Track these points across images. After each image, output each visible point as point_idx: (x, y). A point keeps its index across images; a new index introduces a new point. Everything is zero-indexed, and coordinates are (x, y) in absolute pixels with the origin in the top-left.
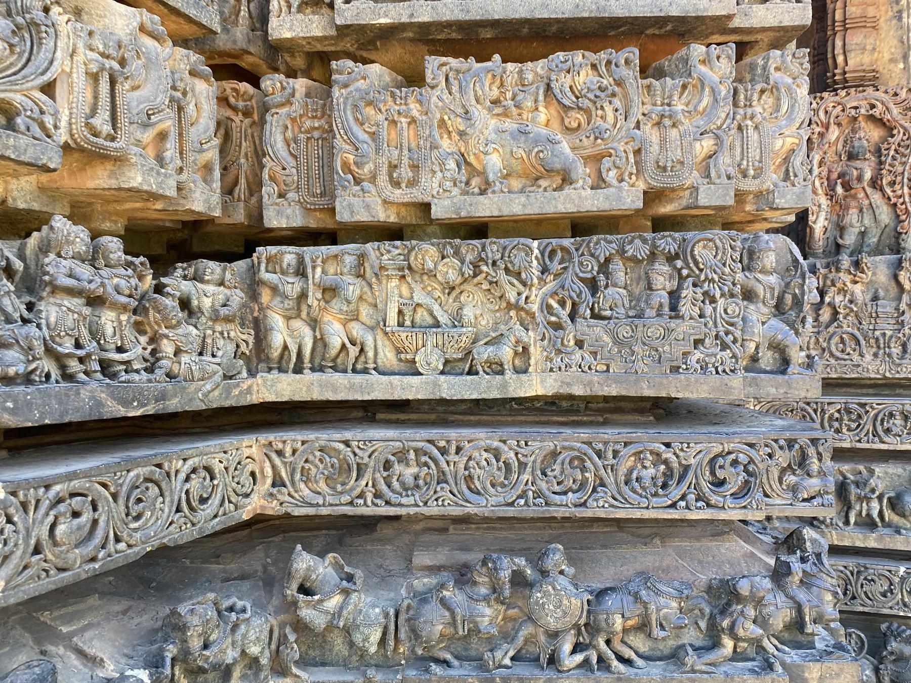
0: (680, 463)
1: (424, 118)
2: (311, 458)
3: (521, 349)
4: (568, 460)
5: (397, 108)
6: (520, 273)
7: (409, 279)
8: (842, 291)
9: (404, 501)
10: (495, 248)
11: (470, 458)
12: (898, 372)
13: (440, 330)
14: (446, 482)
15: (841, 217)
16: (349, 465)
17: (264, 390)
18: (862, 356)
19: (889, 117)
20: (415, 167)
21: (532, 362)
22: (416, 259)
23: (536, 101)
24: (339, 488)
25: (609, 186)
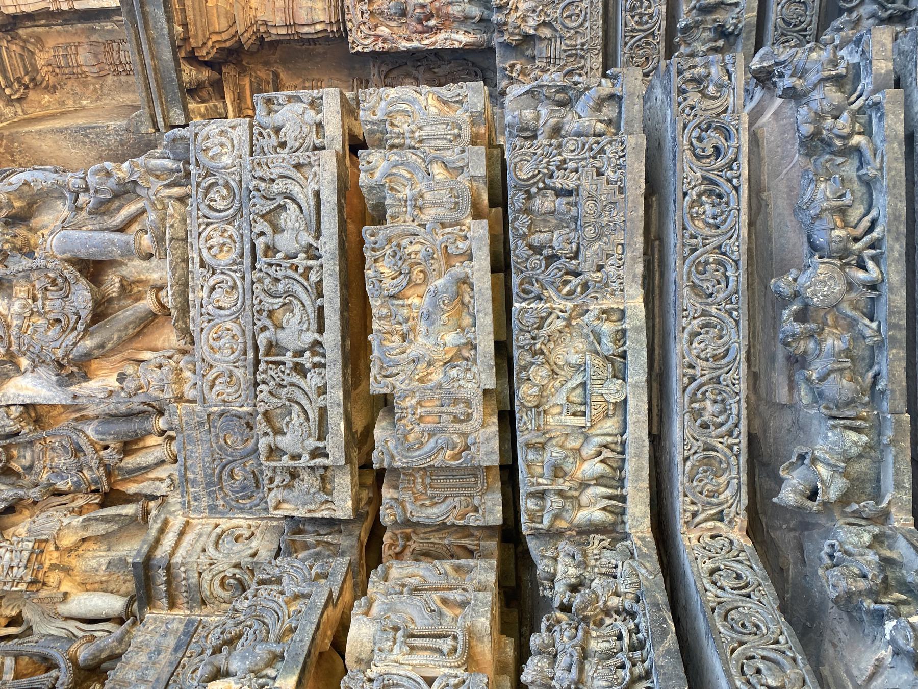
0: (701, 184)
1: (417, 394)
2: (698, 489)
3: (605, 316)
4: (699, 276)
5: (410, 416)
6: (541, 318)
7: (546, 407)
8: (524, 19)
9: (735, 412)
10: (521, 338)
11: (698, 357)
13: (589, 382)
14: (719, 376)
15: (456, 19)
16: (704, 458)
17: (640, 528)
20: (456, 401)
21: (615, 306)
22: (530, 402)
23: (403, 306)
24: (724, 466)
25: (470, 247)
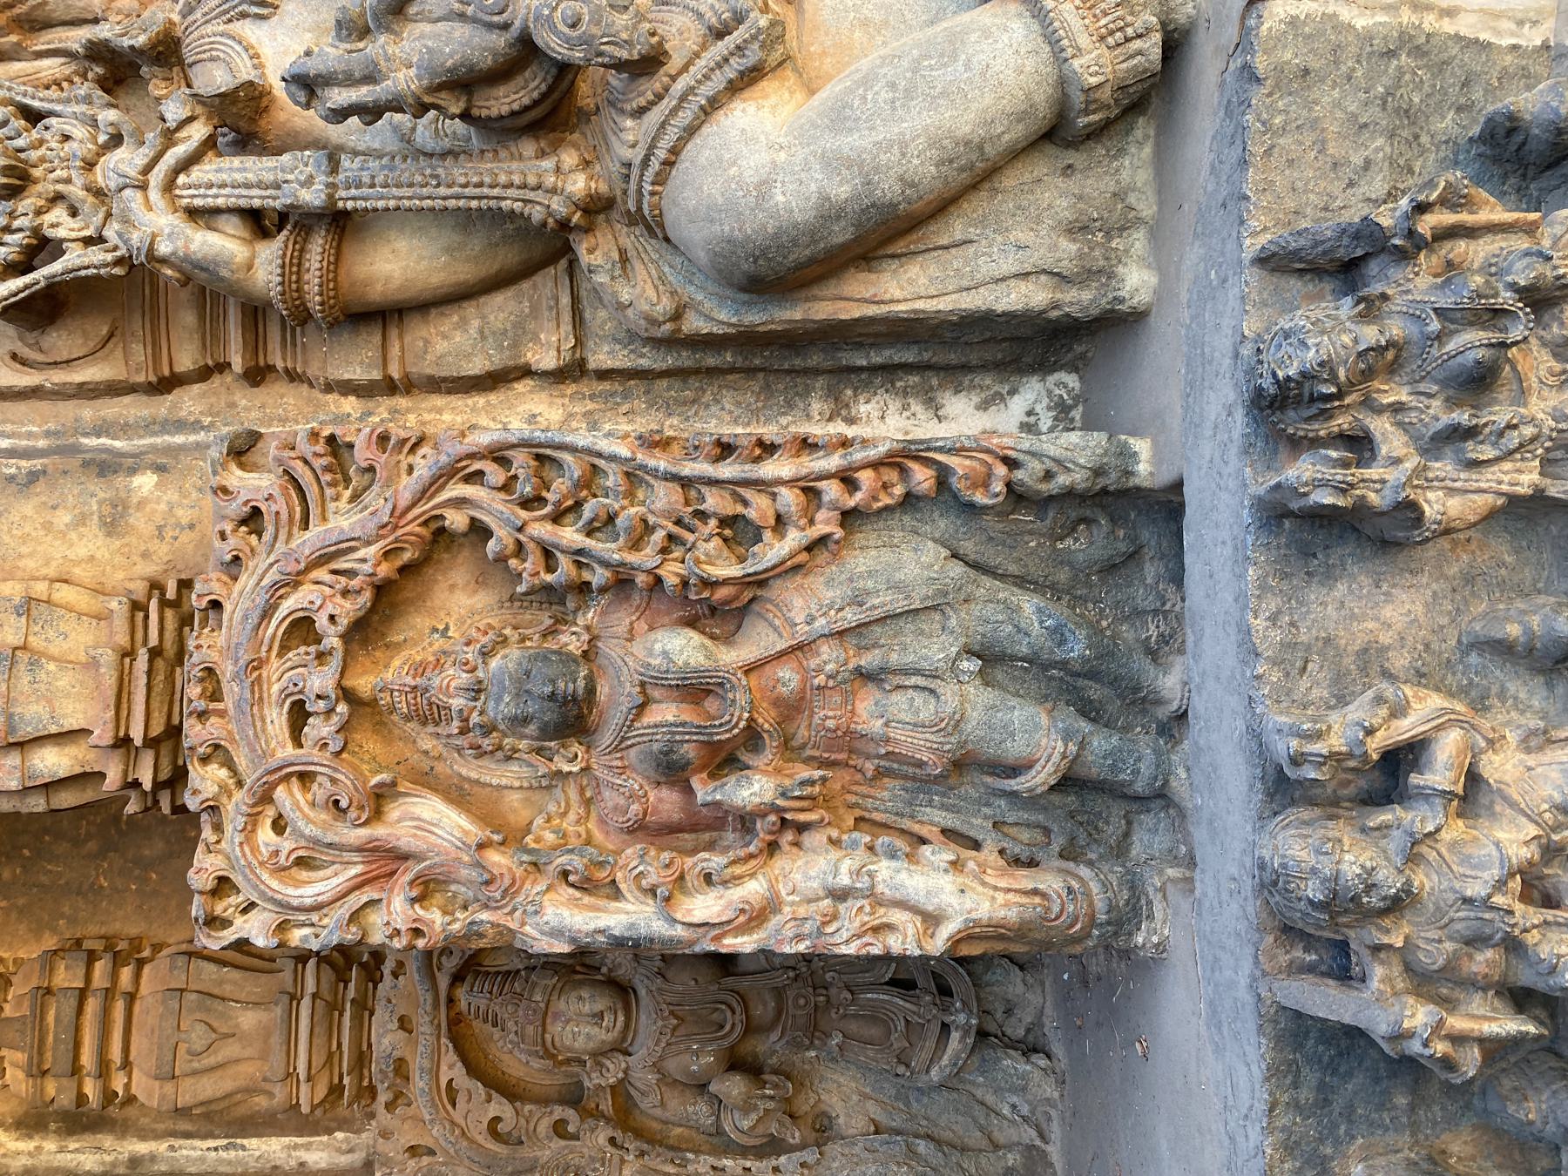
19: (371, 551)
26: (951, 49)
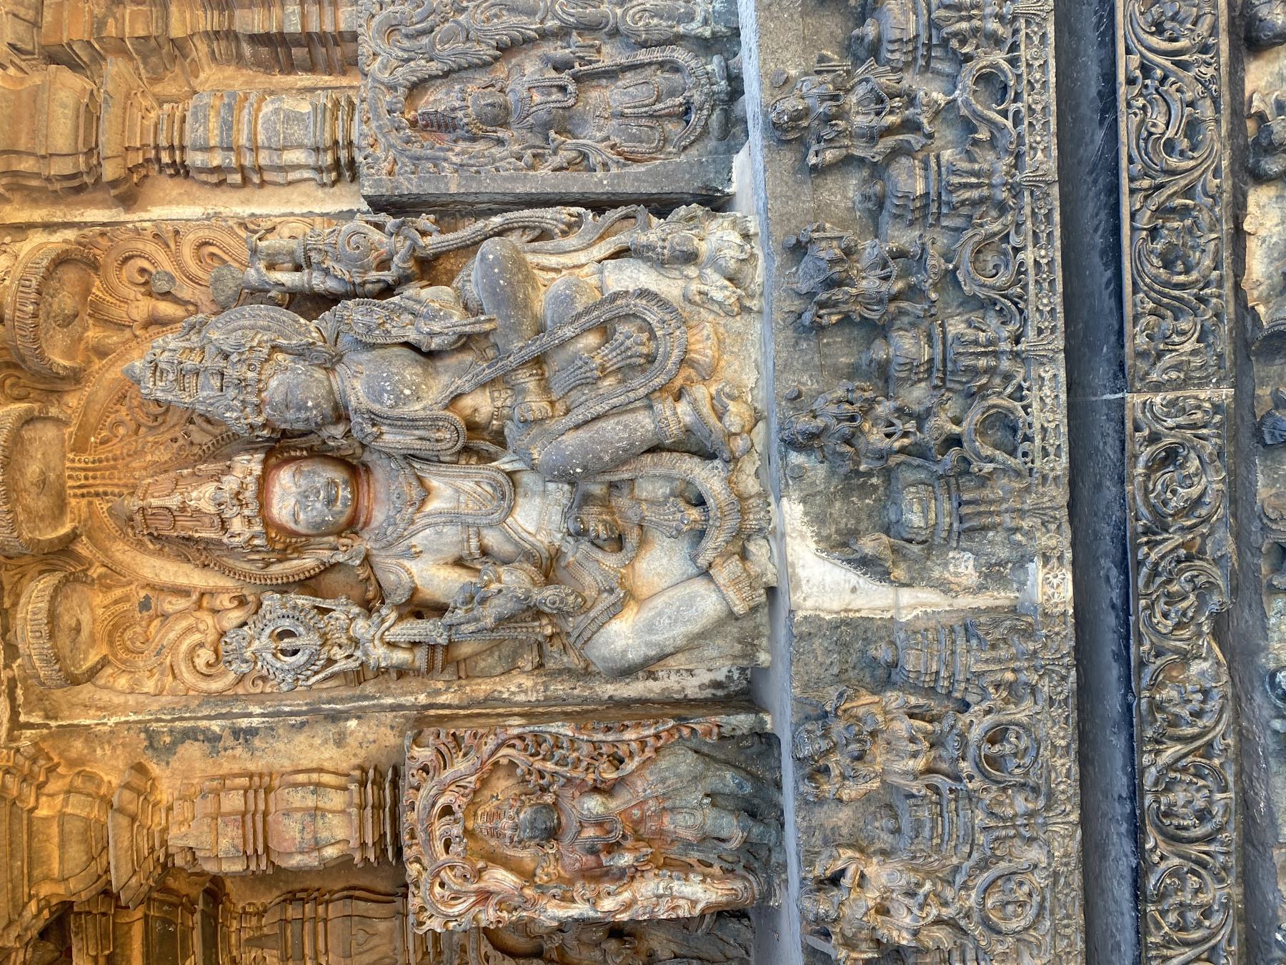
12: (1068, 799)
18: (1036, 866)
19: (473, 779)
26: (690, 601)
